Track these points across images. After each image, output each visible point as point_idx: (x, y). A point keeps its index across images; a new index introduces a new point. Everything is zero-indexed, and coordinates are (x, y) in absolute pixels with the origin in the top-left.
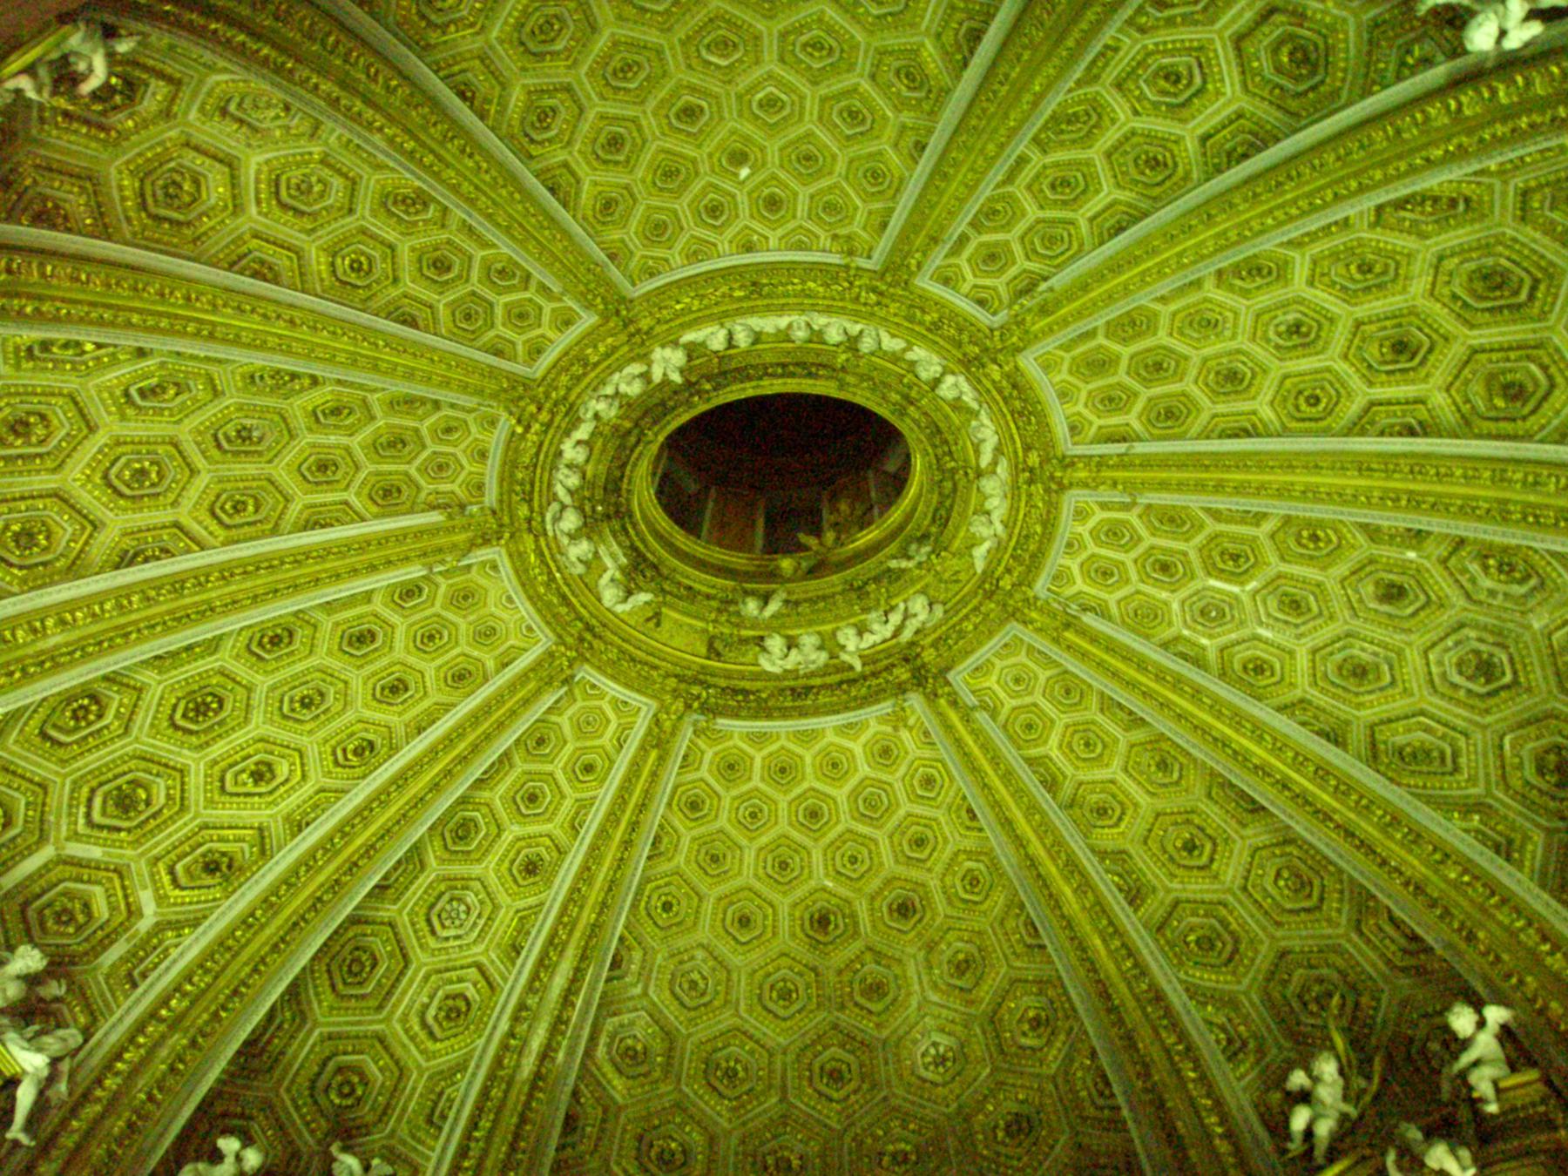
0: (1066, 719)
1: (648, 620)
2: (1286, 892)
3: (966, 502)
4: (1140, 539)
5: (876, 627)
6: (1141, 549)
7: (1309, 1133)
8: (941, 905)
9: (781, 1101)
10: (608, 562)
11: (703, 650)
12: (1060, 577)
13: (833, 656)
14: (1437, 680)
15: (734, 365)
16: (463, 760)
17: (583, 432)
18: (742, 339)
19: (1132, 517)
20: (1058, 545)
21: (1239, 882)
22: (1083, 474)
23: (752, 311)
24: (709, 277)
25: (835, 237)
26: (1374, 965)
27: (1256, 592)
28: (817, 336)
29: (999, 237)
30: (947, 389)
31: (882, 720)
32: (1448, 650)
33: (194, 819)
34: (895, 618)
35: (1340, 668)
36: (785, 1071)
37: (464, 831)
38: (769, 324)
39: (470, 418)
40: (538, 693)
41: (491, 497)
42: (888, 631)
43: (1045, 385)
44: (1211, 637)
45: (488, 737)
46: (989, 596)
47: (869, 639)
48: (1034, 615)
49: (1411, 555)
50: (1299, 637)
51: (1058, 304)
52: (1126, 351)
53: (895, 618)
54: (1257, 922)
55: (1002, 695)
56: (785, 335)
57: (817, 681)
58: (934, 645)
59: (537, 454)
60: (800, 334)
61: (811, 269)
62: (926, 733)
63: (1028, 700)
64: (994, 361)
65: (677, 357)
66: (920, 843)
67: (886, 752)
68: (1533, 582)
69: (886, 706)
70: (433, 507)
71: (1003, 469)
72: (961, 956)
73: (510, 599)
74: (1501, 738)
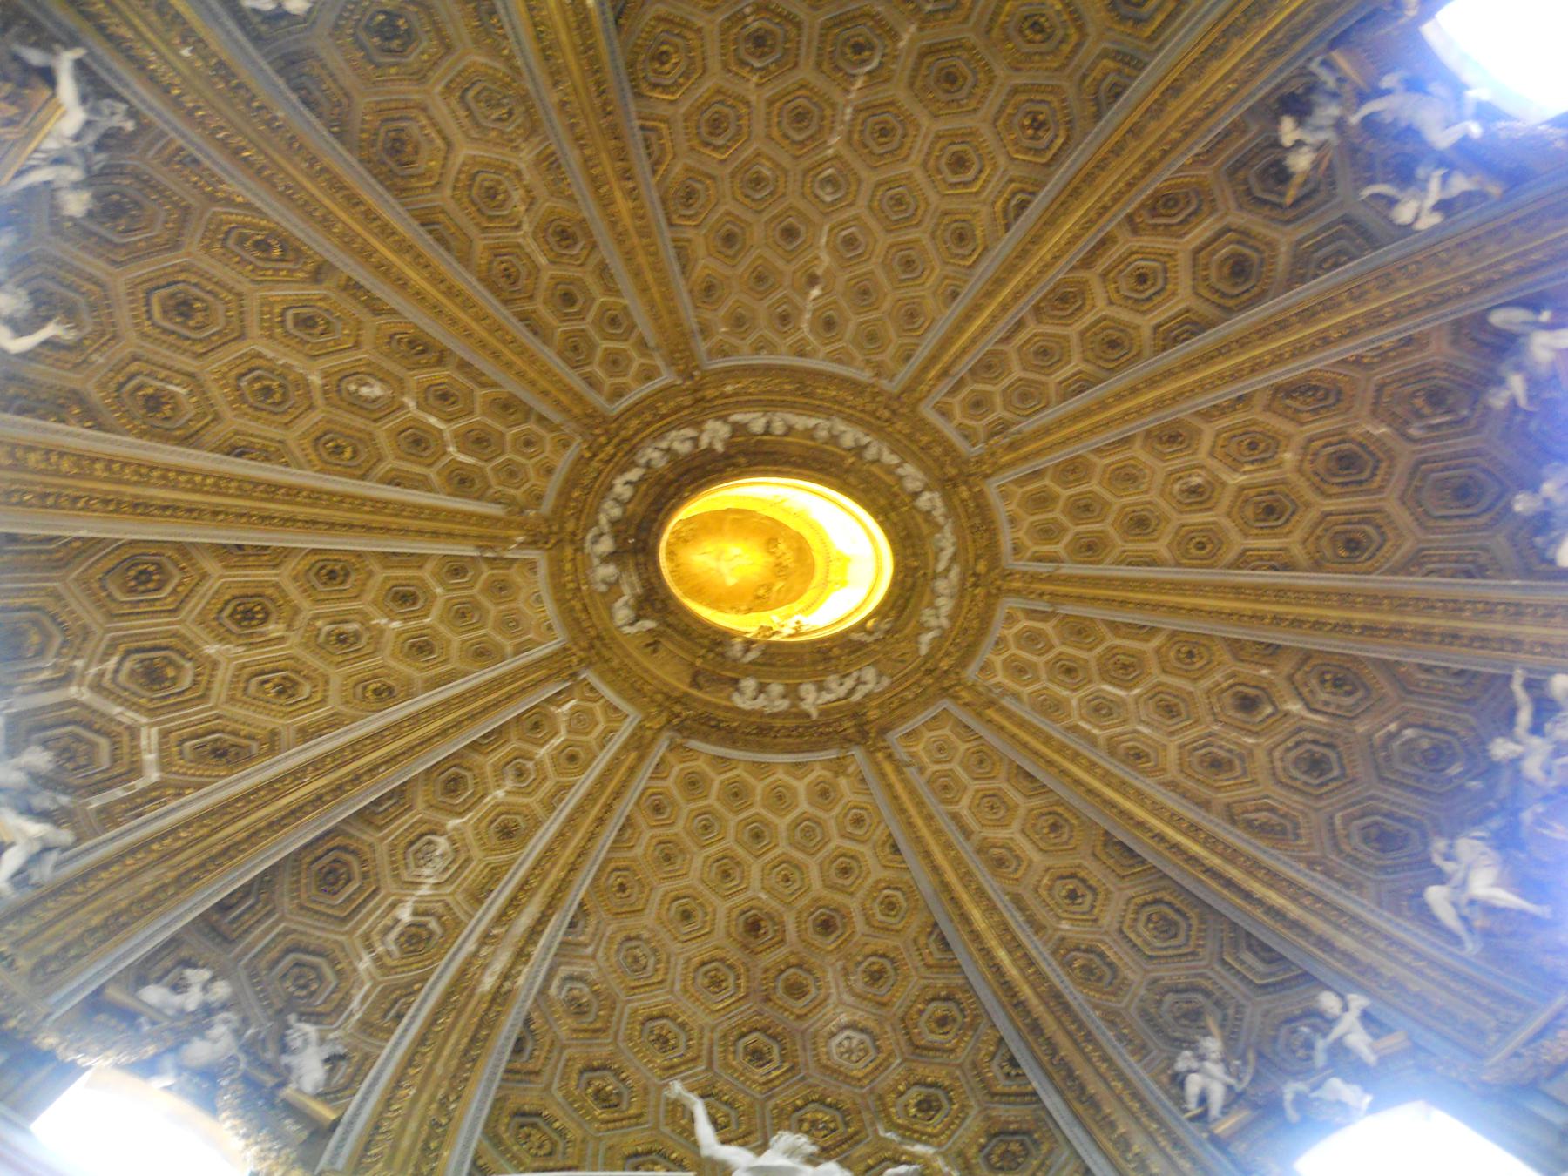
0: (977, 785)
1: (648, 645)
3: (921, 596)
4: (1052, 647)
5: (834, 686)
6: (1051, 655)
8: (860, 925)
9: (706, 1070)
10: (626, 589)
11: (688, 680)
12: (986, 668)
13: (793, 705)
14: (1280, 773)
15: (766, 448)
16: (473, 717)
17: (634, 475)
18: (778, 427)
19: (1048, 627)
20: (990, 640)
21: (1116, 926)
22: (1016, 585)
23: (791, 406)
24: (768, 369)
25: (868, 362)
27: (1139, 696)
28: (834, 439)
29: (988, 388)
30: (924, 501)
31: (827, 764)
32: (1288, 750)
33: (211, 708)
34: (849, 683)
36: (711, 1046)
37: (454, 785)
38: (802, 422)
39: (549, 437)
40: (547, 679)
41: (547, 507)
42: (842, 691)
43: (1002, 511)
44: (1102, 728)
45: (496, 704)
46: (929, 672)
47: (827, 697)
48: (963, 694)
49: (1265, 672)
50: (1172, 733)
51: (1024, 442)
52: (1065, 493)
53: (849, 683)
55: (926, 760)
56: (809, 433)
57: (778, 723)
58: (880, 706)
59: (596, 478)
60: (823, 434)
61: (844, 382)
62: (863, 780)
63: (947, 766)
64: (965, 483)
65: (723, 430)
66: (845, 871)
67: (824, 793)
68: (1360, 694)
69: (831, 754)
70: (496, 501)
71: (954, 574)
72: (876, 967)
73: (539, 600)
74: (1331, 817)
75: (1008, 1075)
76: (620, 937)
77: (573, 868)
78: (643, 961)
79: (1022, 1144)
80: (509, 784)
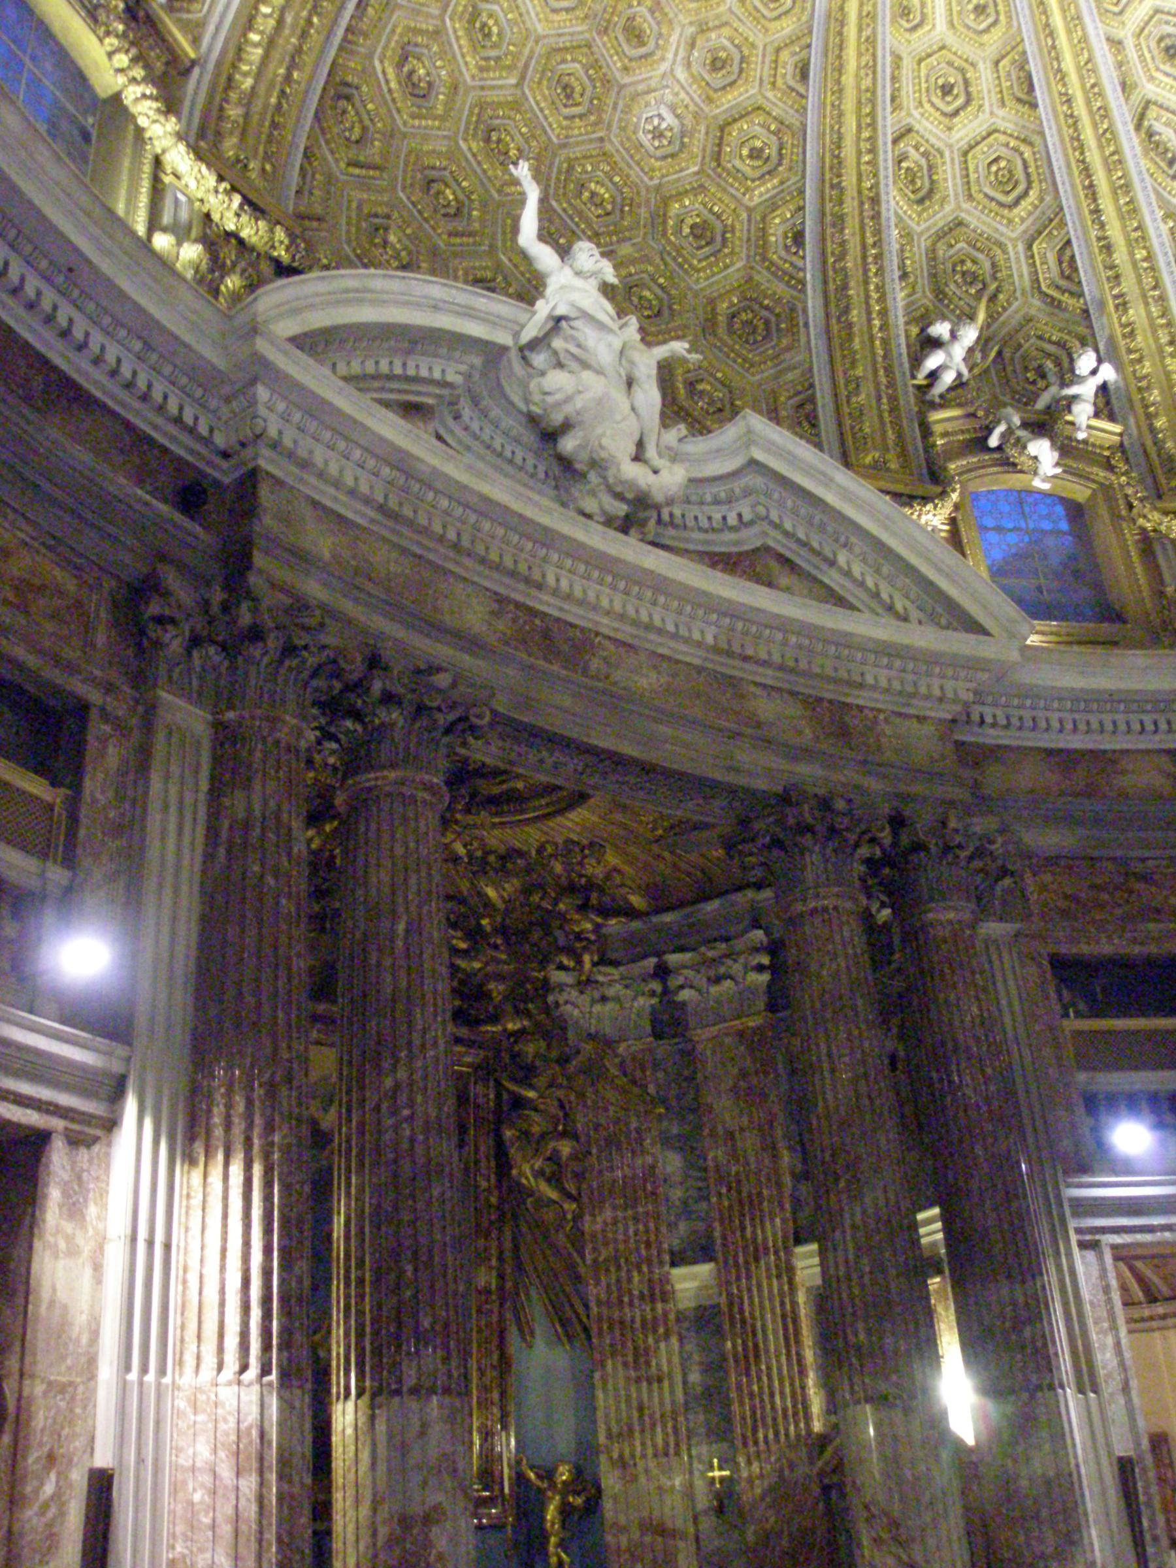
2: (992, 178)
7: (933, 376)
9: (517, 85)
21: (963, 144)
26: (1021, 276)
35: (1161, 39)
36: (530, 58)
54: (955, 185)
72: (723, 55)
75: (786, 247)
79: (767, 322)
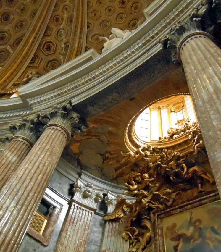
76: (99, 23)
77: (82, 18)
78: (106, 24)
80: (66, 13)
